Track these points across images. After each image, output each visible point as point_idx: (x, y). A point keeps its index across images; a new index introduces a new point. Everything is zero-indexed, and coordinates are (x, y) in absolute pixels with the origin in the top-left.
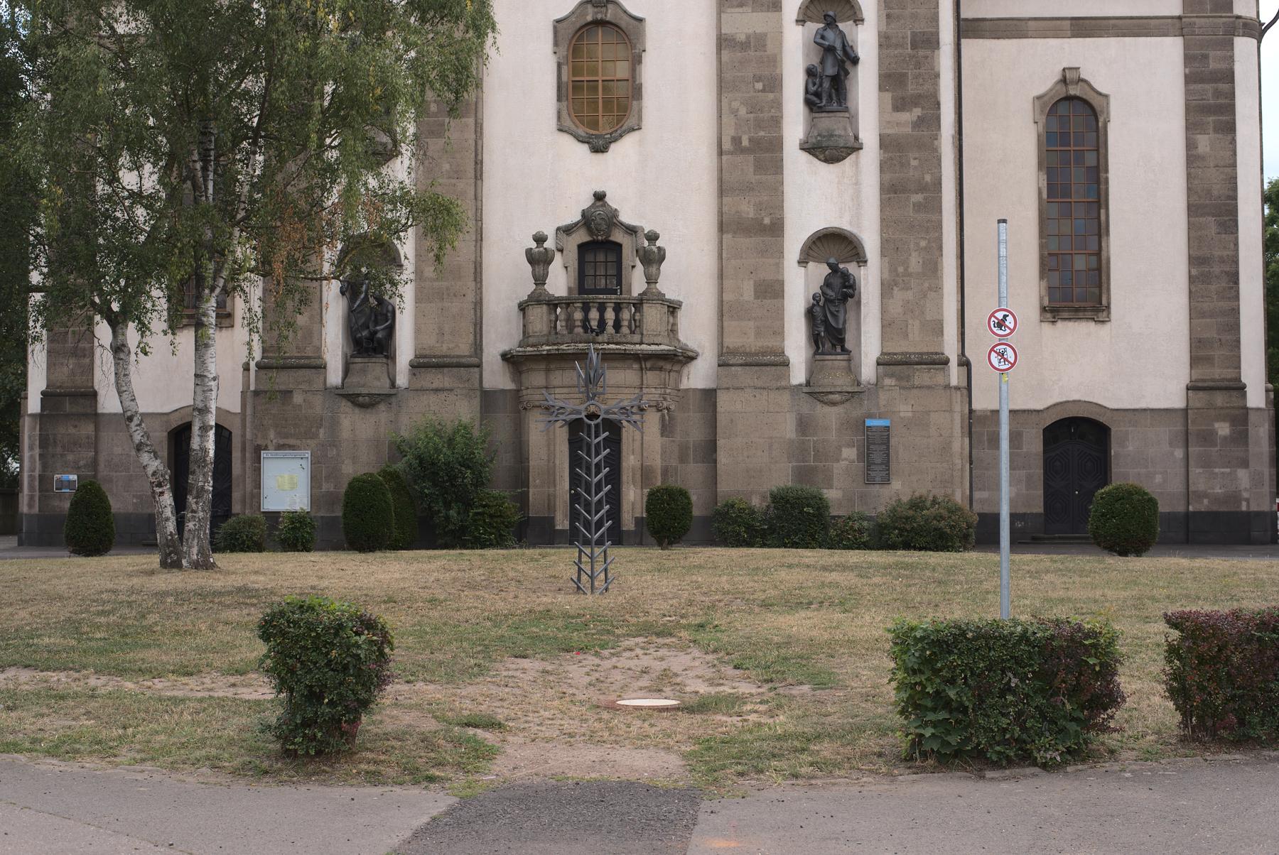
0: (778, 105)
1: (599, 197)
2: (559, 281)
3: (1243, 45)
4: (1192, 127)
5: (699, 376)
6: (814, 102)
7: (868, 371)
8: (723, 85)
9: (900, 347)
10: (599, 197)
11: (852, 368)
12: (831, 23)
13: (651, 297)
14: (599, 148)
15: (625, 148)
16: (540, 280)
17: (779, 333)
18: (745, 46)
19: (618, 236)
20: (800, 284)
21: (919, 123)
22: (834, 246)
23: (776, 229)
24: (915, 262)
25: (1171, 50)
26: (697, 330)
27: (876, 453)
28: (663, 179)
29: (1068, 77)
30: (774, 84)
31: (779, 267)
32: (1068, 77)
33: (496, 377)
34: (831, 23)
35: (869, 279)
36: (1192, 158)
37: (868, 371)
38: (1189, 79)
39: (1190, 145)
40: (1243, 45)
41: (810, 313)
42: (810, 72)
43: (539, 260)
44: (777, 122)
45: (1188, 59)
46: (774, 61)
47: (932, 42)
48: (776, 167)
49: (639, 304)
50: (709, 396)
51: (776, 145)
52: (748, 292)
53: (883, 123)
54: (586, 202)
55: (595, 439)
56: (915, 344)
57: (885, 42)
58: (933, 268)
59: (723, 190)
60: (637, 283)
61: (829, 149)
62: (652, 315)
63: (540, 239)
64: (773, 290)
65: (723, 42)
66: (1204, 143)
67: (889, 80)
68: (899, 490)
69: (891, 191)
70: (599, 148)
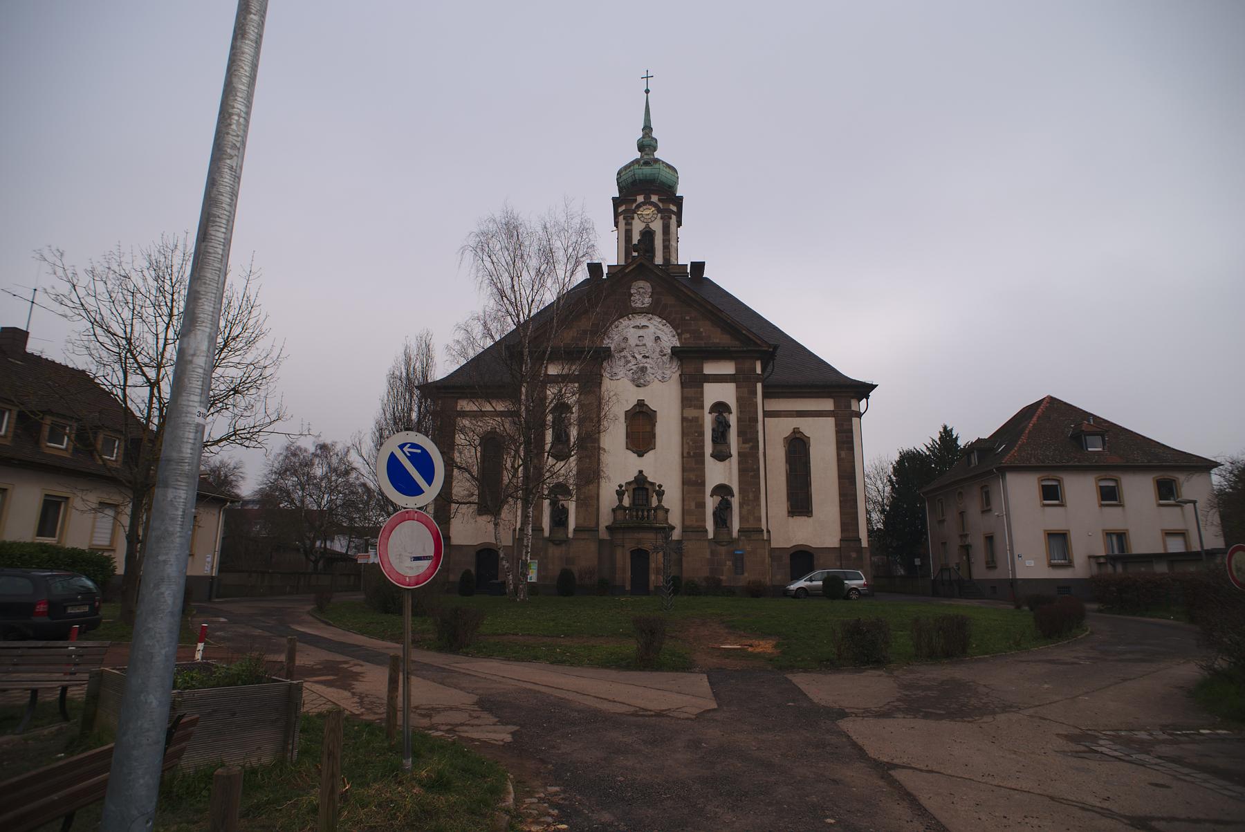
0: (703, 441)
1: (641, 472)
2: (626, 502)
3: (855, 420)
4: (839, 448)
5: (676, 535)
6: (714, 441)
7: (735, 534)
8: (684, 434)
9: (746, 526)
10: (641, 472)
11: (730, 533)
12: (720, 413)
13: (660, 507)
14: (641, 455)
15: (650, 456)
16: (621, 500)
17: (704, 520)
18: (691, 421)
19: (647, 486)
20: (711, 503)
21: (751, 448)
22: (722, 490)
23: (703, 484)
24: (751, 496)
25: (831, 421)
26: (675, 519)
27: (739, 563)
28: (663, 466)
29: (796, 431)
30: (702, 434)
31: (704, 498)
32: (796, 431)
33: (603, 534)
34: (720, 413)
35: (735, 502)
36: (839, 460)
37: (735, 534)
38: (837, 432)
39: (838, 455)
40: (855, 420)
41: (714, 514)
42: (713, 430)
43: (620, 494)
44: (702, 447)
45: (837, 425)
46: (702, 426)
47: (756, 421)
48: (703, 462)
49: (655, 509)
50: (679, 542)
51: (703, 455)
53: (739, 448)
54: (636, 474)
55: (640, 557)
56: (751, 524)
57: (739, 420)
58: (757, 498)
59: (684, 470)
60: (654, 503)
61: (721, 456)
62: (660, 514)
63: (620, 486)
64: (702, 505)
65: (684, 419)
66: (843, 454)
67: (740, 433)
68: (747, 577)
69: (742, 471)
70: (641, 455)
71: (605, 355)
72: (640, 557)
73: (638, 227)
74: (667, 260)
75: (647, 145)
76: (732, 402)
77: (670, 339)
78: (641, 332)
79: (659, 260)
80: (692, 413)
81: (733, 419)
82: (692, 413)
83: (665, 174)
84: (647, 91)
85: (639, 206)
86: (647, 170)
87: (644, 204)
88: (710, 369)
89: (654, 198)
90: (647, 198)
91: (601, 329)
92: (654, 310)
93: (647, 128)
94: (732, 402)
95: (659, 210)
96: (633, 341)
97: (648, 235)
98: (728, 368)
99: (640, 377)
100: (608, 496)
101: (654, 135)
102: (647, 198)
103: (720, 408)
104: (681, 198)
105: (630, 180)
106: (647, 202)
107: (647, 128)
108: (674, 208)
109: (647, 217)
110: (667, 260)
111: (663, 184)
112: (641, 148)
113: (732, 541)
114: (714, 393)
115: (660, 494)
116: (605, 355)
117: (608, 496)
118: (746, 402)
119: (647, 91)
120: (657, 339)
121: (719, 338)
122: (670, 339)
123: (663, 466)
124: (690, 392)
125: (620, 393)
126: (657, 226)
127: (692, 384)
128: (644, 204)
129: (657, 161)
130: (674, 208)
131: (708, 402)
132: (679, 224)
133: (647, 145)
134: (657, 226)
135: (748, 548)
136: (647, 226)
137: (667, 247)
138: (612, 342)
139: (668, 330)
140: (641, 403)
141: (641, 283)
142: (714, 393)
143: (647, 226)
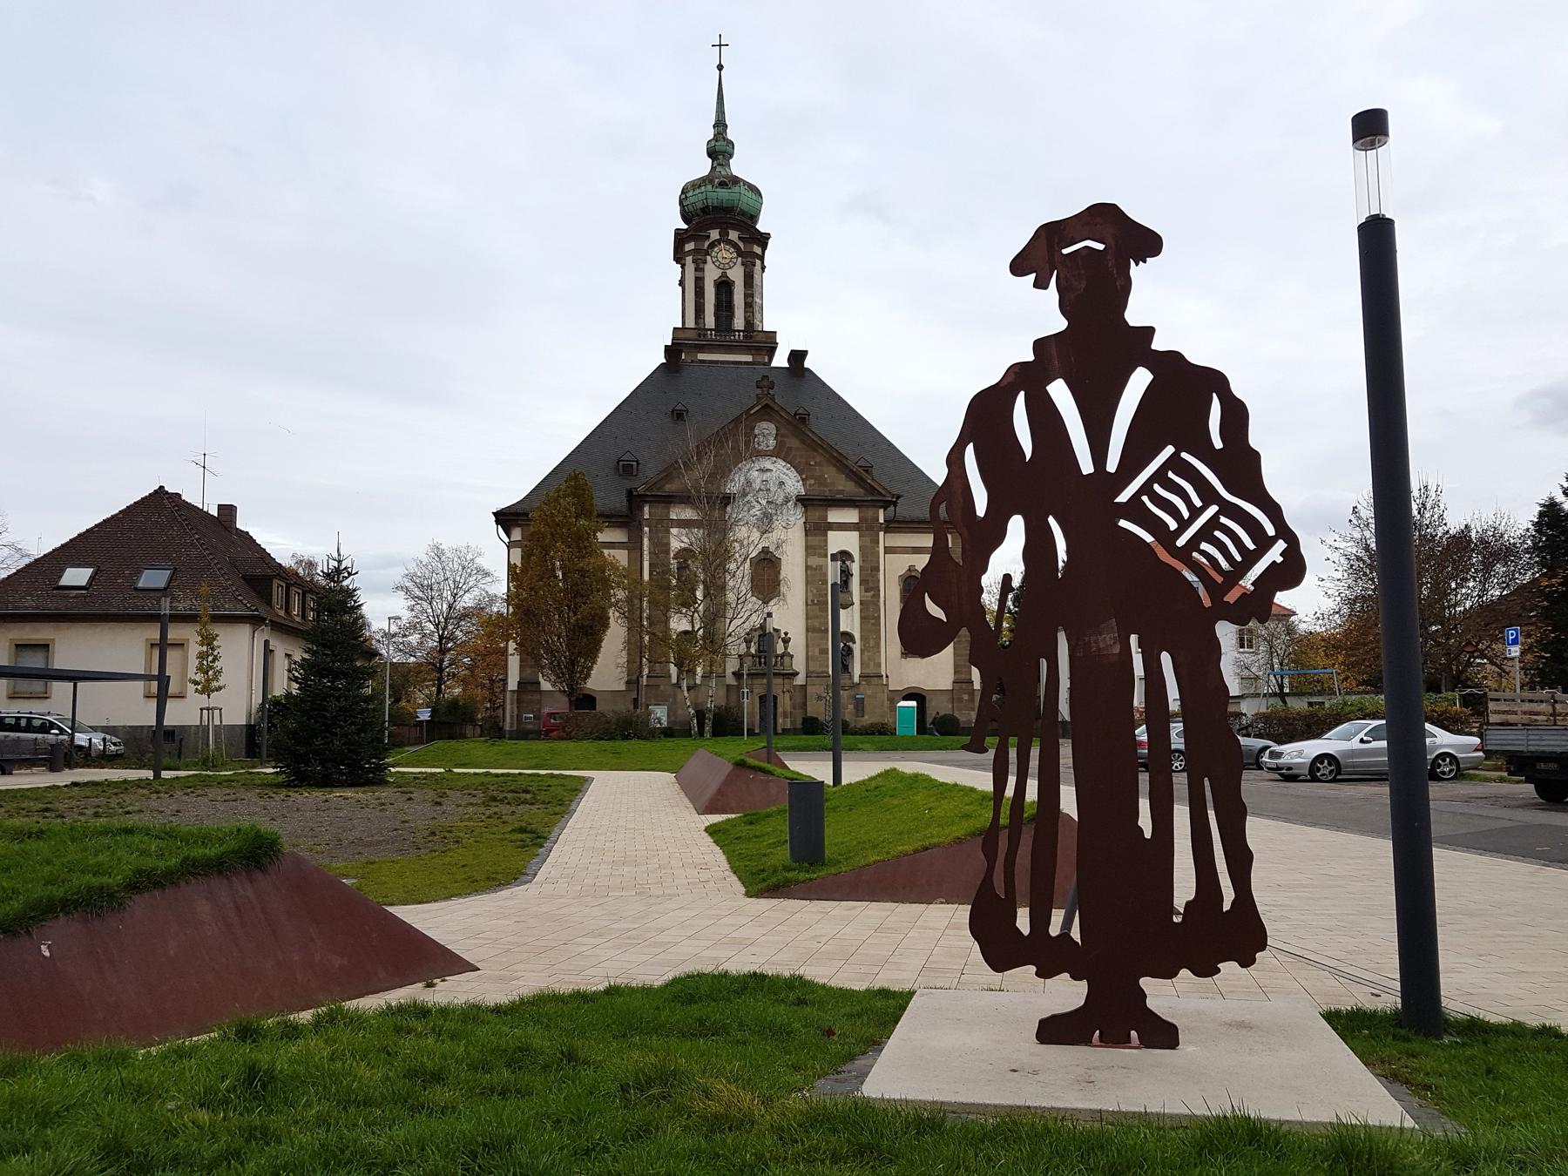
5: (800, 680)
7: (856, 679)
9: (867, 671)
11: (851, 678)
26: (799, 664)
27: (860, 706)
28: (789, 616)
37: (856, 679)
46: (826, 574)
49: (782, 656)
50: (804, 687)
52: (817, 652)
55: (767, 702)
56: (871, 670)
58: (878, 645)
60: (780, 649)
62: (787, 659)
65: (807, 567)
68: (867, 720)
71: (727, 500)
72: (767, 702)
73: (711, 274)
74: (749, 324)
75: (720, 150)
76: (856, 554)
77: (794, 484)
78: (766, 476)
79: (739, 323)
80: (815, 561)
81: (855, 568)
82: (815, 561)
83: (747, 198)
84: (720, 67)
85: (712, 245)
86: (723, 194)
87: (719, 241)
88: (834, 516)
89: (733, 235)
90: (724, 234)
91: (723, 471)
92: (780, 452)
93: (720, 125)
94: (856, 554)
95: (740, 253)
96: (757, 485)
97: (724, 286)
98: (851, 516)
99: (766, 523)
100: (736, 647)
101: (730, 135)
102: (724, 234)
103: (844, 556)
104: (766, 237)
105: (700, 205)
106: (724, 239)
107: (720, 125)
108: (758, 250)
109: (722, 262)
110: (749, 324)
111: (743, 213)
112: (712, 153)
113: (855, 686)
114: (838, 541)
115: (786, 641)
116: (727, 500)
117: (736, 647)
118: (869, 553)
119: (720, 67)
120: (782, 483)
121: (846, 486)
122: (794, 484)
123: (789, 616)
124: (814, 540)
125: (747, 538)
126: (736, 275)
127: (816, 531)
128: (719, 241)
129: (736, 181)
130: (758, 250)
131: (833, 549)
132: (763, 268)
133: (720, 150)
134: (736, 275)
135: (869, 693)
136: (724, 275)
137: (749, 305)
138: (732, 487)
139: (793, 473)
140: (765, 550)
141: (765, 425)
142: (838, 541)
143: (724, 275)
